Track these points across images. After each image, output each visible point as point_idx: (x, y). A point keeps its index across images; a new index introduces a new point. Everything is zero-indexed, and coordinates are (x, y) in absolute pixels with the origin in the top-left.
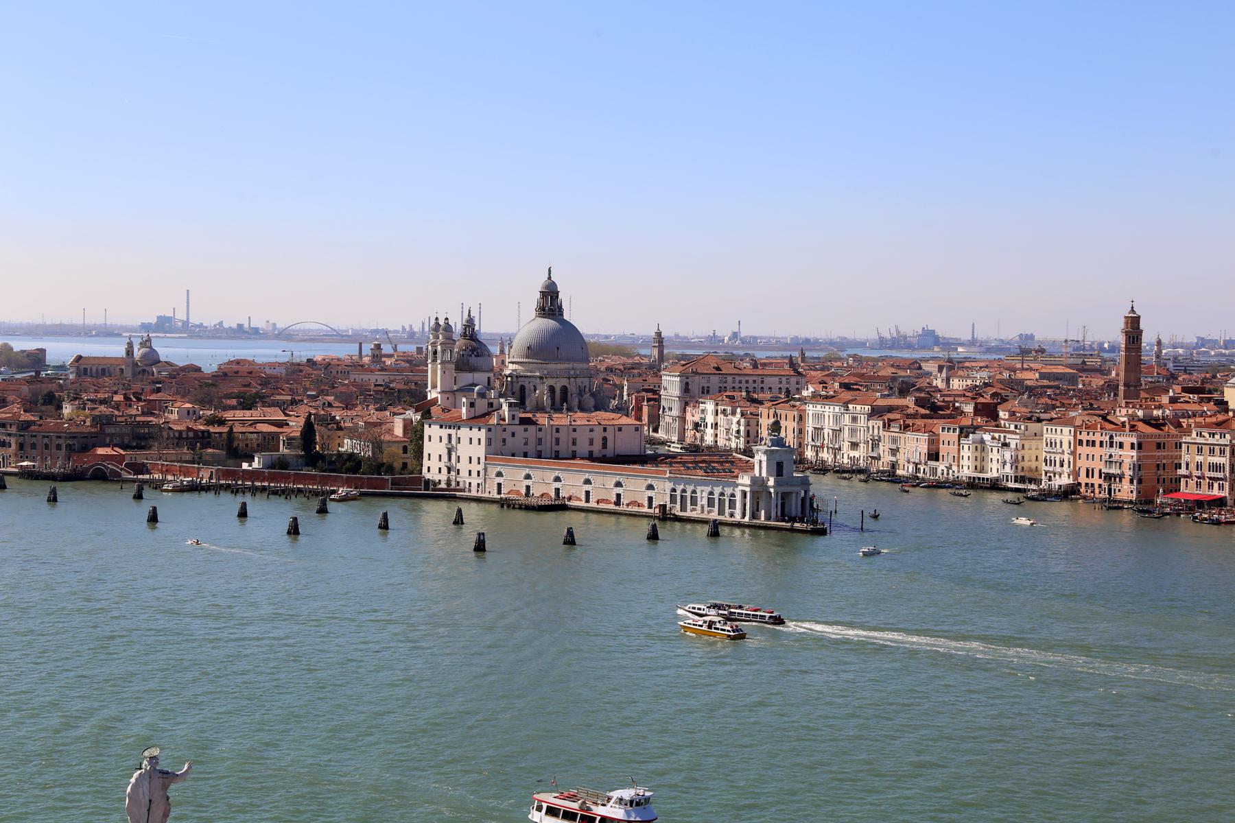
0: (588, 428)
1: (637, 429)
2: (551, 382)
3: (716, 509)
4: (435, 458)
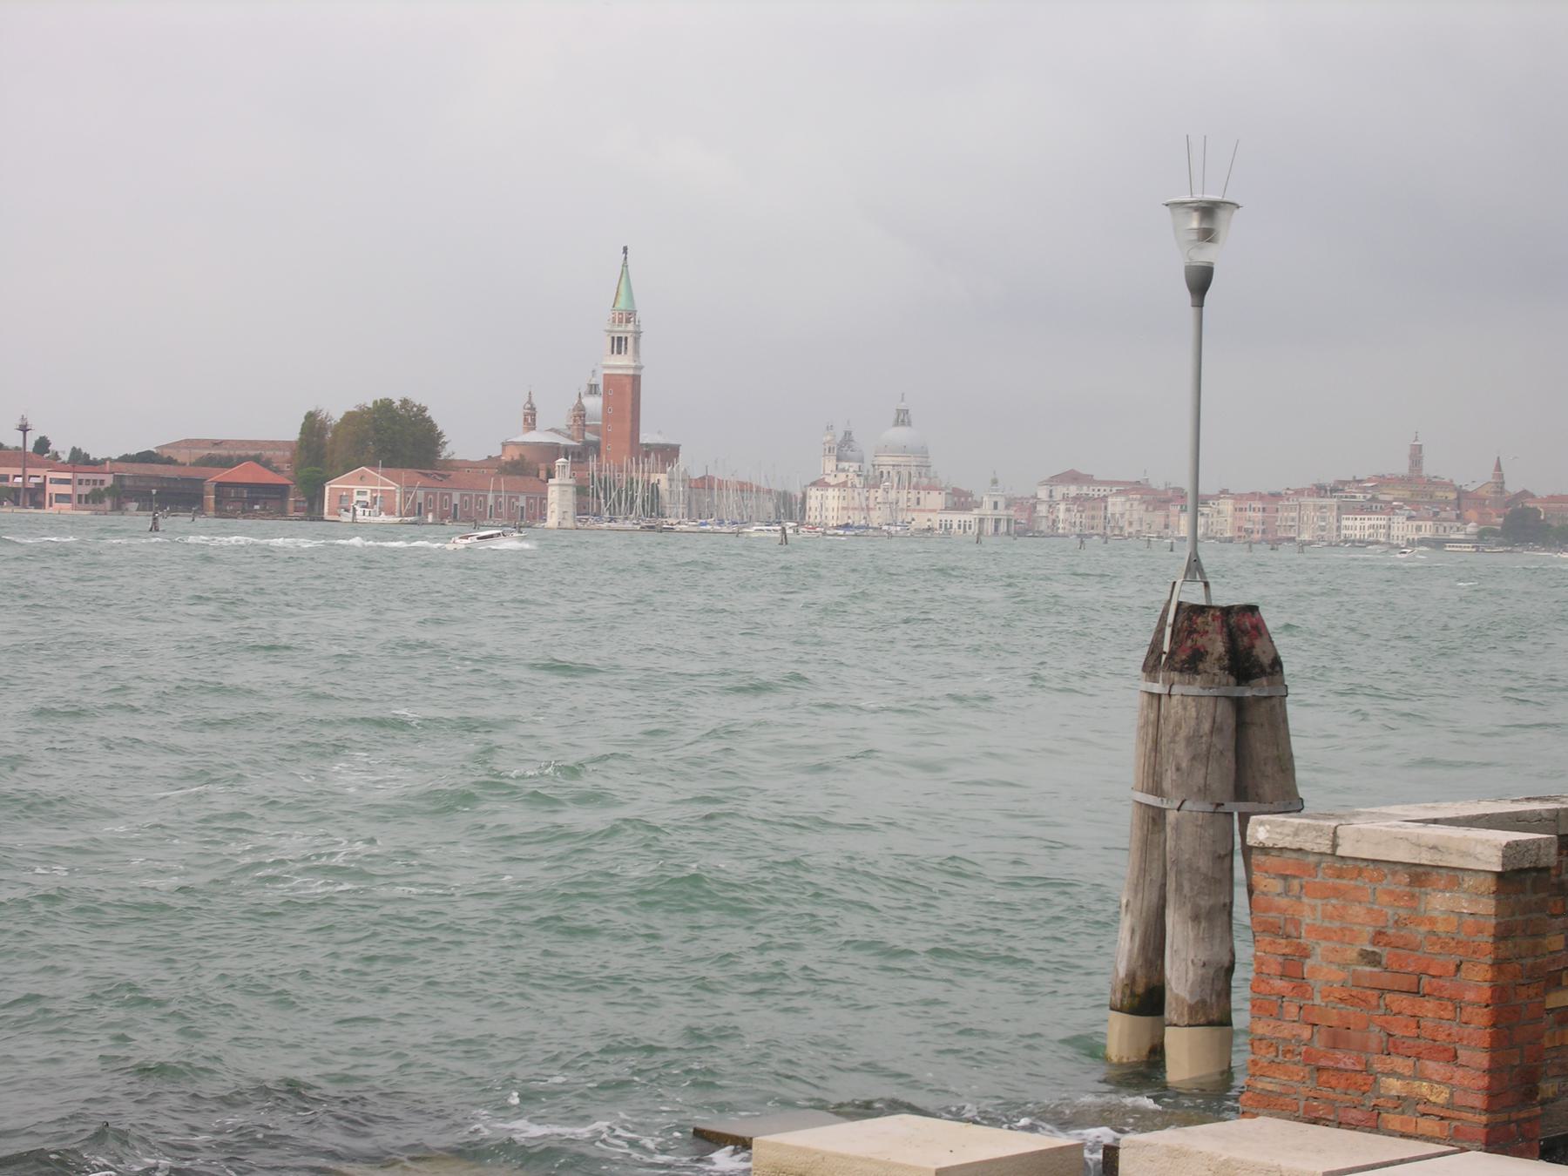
4: (813, 509)
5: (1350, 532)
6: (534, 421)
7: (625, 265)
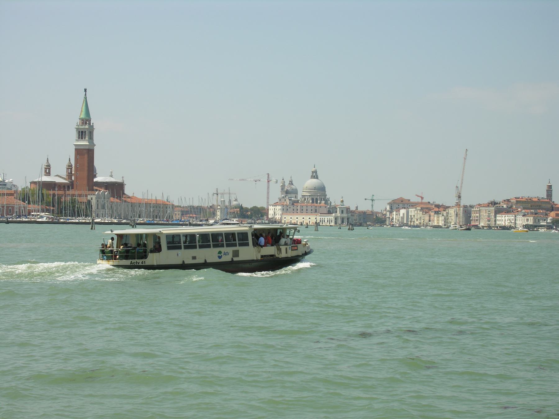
0: (311, 206)
1: (325, 207)
2: (313, 197)
3: (329, 223)
5: (500, 222)
6: (49, 171)
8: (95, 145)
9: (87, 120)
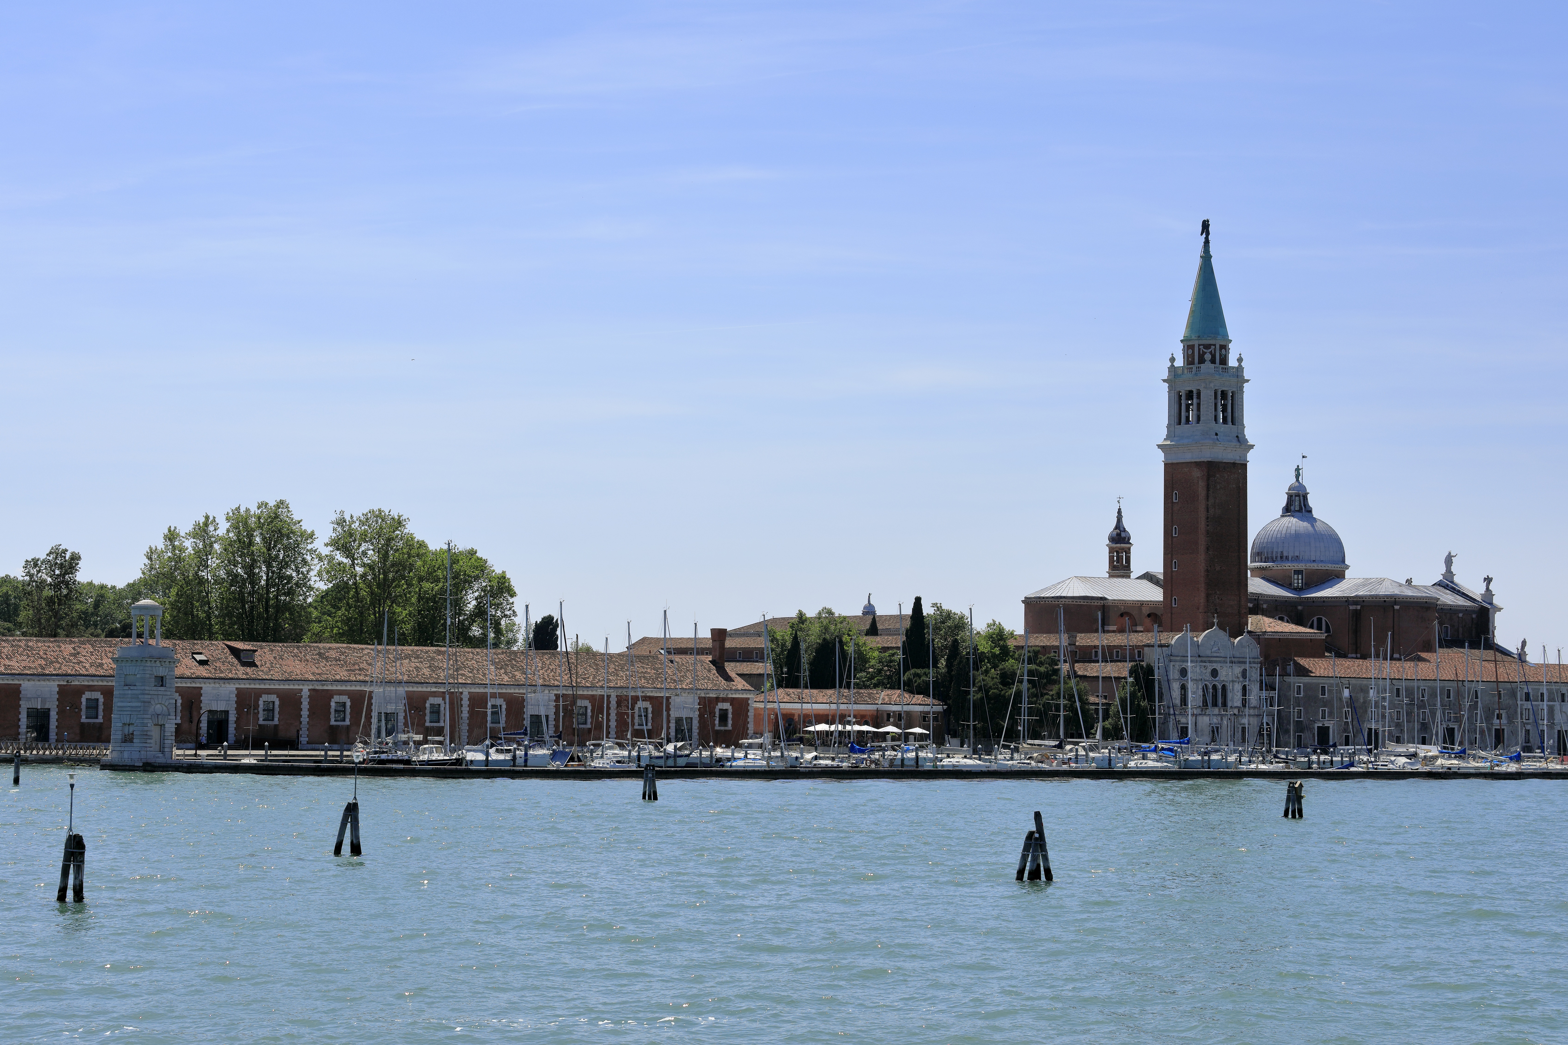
7: (1206, 257)
8: (1252, 446)
9: (1207, 347)
